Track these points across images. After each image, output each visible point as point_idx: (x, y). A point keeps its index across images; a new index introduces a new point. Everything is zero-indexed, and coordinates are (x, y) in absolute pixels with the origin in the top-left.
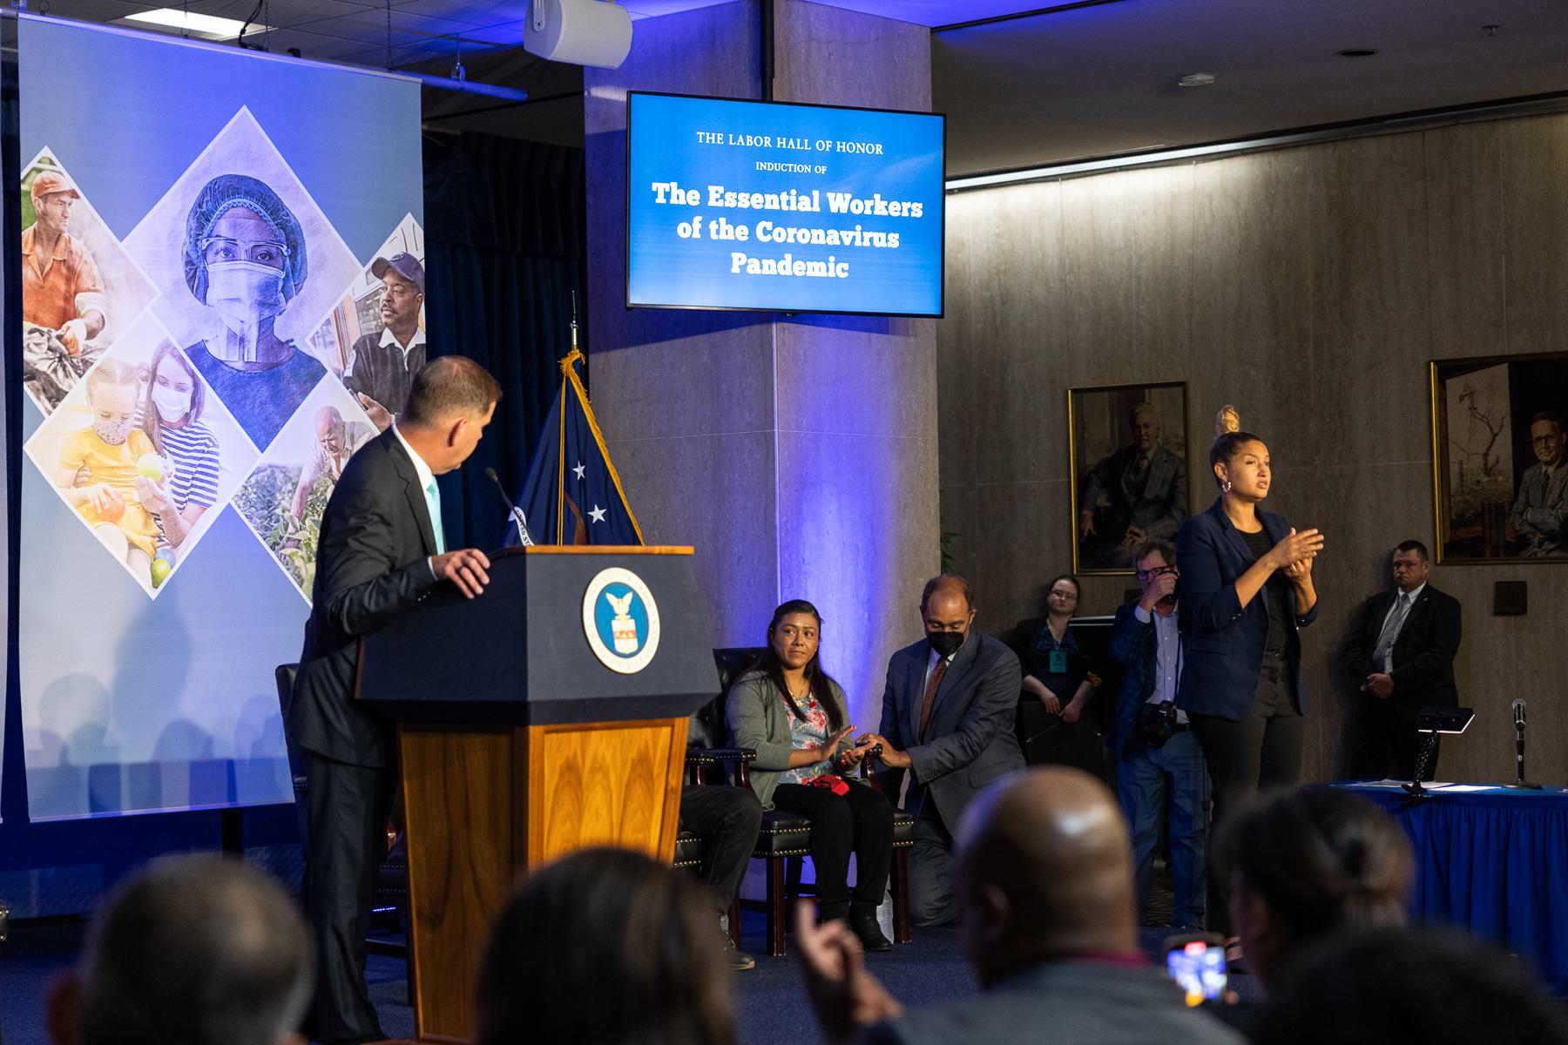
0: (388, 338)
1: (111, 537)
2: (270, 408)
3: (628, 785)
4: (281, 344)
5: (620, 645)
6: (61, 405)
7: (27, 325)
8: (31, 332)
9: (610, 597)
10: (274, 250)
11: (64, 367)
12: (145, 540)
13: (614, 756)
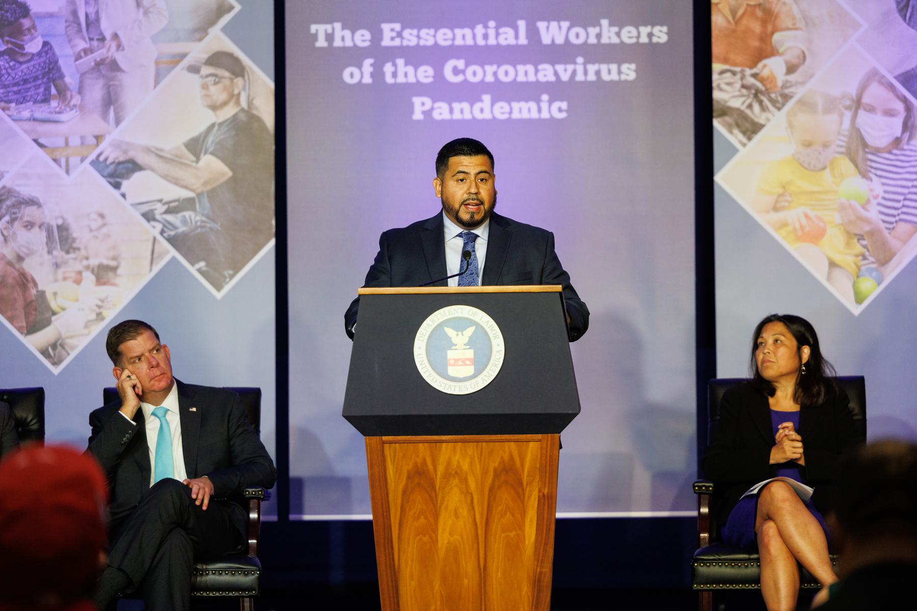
1: (811, 259)
3: (491, 490)
5: (452, 371)
6: (757, 138)
7: (716, 67)
8: (722, 72)
9: (450, 332)
11: (761, 103)
12: (847, 259)
13: (471, 464)
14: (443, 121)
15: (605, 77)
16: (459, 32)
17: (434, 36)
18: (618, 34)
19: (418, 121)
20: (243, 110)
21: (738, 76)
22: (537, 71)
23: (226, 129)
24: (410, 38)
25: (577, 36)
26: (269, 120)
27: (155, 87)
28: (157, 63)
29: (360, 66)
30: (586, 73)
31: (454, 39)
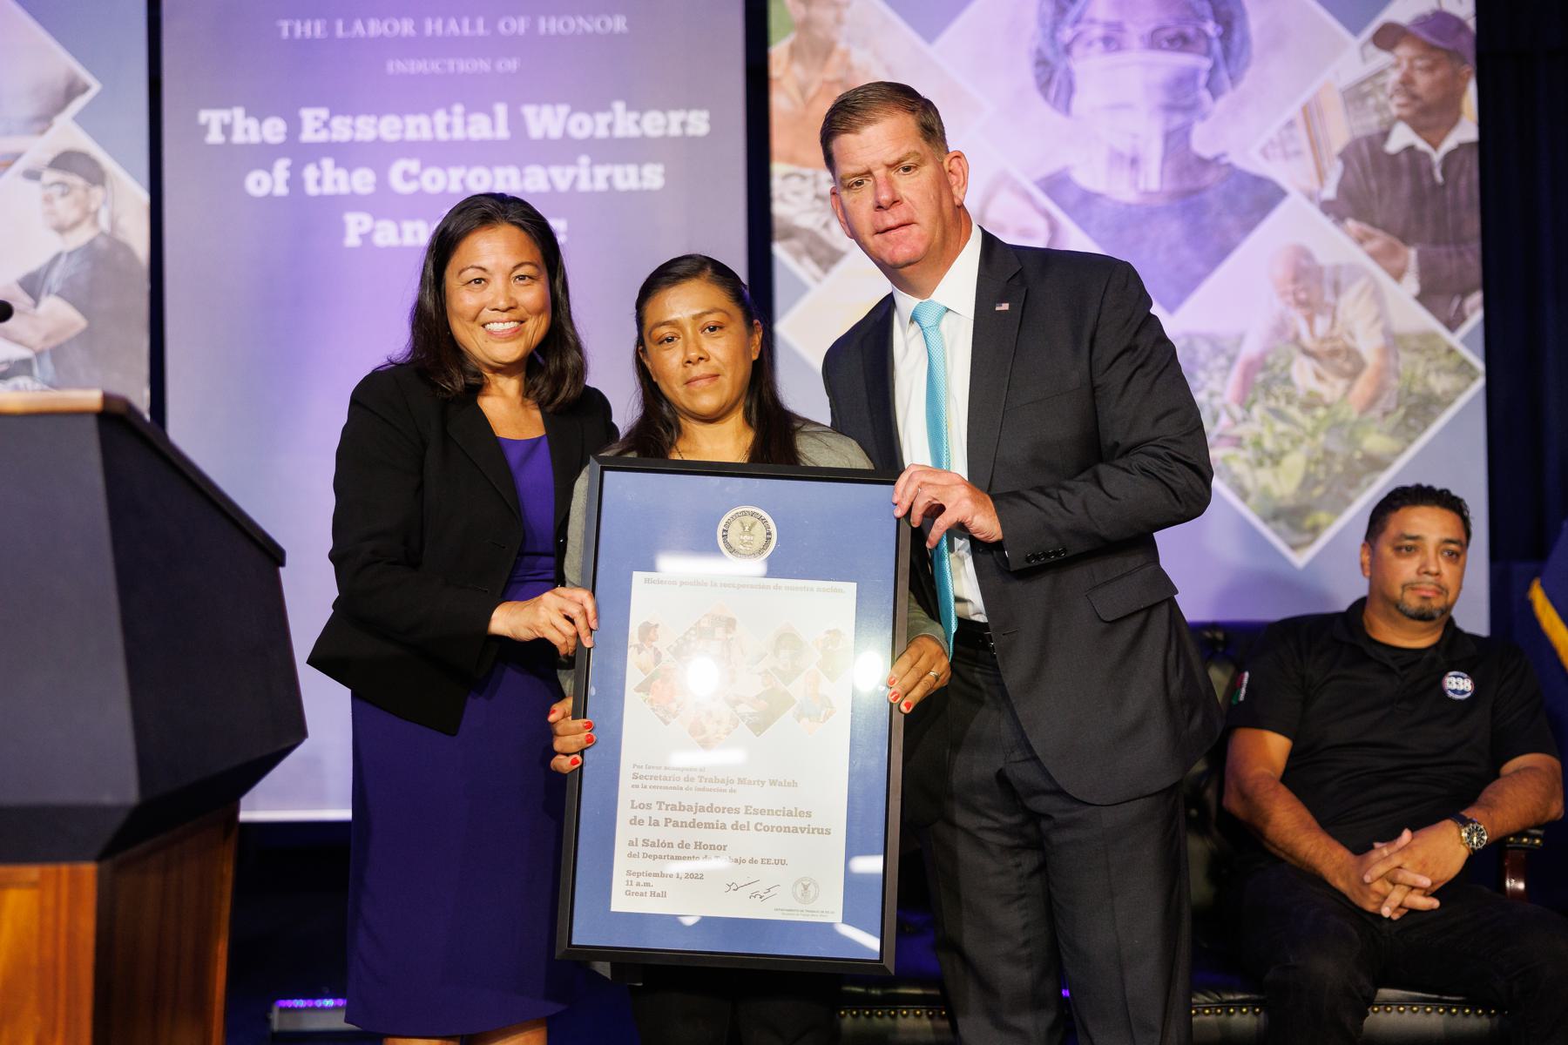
0: (1402, 138)
2: (1186, 253)
4: (1204, 163)
7: (778, 169)
8: (787, 176)
10: (1190, 31)
14: (389, 250)
15: (621, 184)
16: (411, 121)
17: (376, 127)
18: (638, 123)
19: (353, 249)
20: (102, 233)
21: (810, 183)
22: (522, 176)
24: (342, 129)
25: (580, 126)
26: (142, 248)
29: (269, 170)
30: (592, 178)
31: (403, 131)
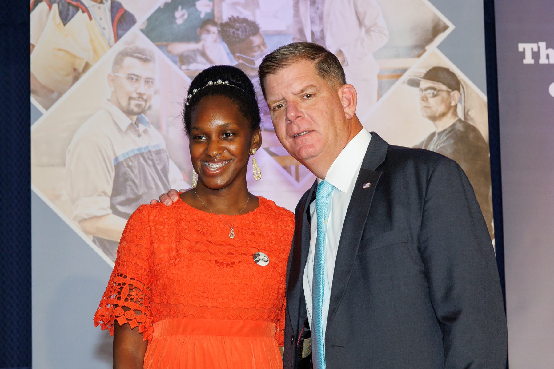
20: (460, 120)
23: (445, 138)
26: (484, 130)
27: (378, 100)
28: (379, 77)
